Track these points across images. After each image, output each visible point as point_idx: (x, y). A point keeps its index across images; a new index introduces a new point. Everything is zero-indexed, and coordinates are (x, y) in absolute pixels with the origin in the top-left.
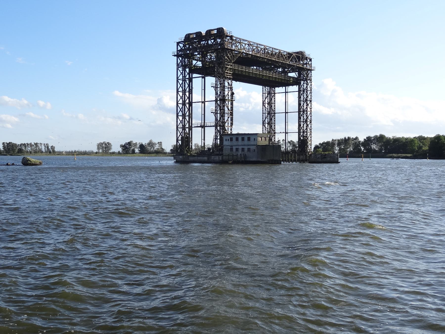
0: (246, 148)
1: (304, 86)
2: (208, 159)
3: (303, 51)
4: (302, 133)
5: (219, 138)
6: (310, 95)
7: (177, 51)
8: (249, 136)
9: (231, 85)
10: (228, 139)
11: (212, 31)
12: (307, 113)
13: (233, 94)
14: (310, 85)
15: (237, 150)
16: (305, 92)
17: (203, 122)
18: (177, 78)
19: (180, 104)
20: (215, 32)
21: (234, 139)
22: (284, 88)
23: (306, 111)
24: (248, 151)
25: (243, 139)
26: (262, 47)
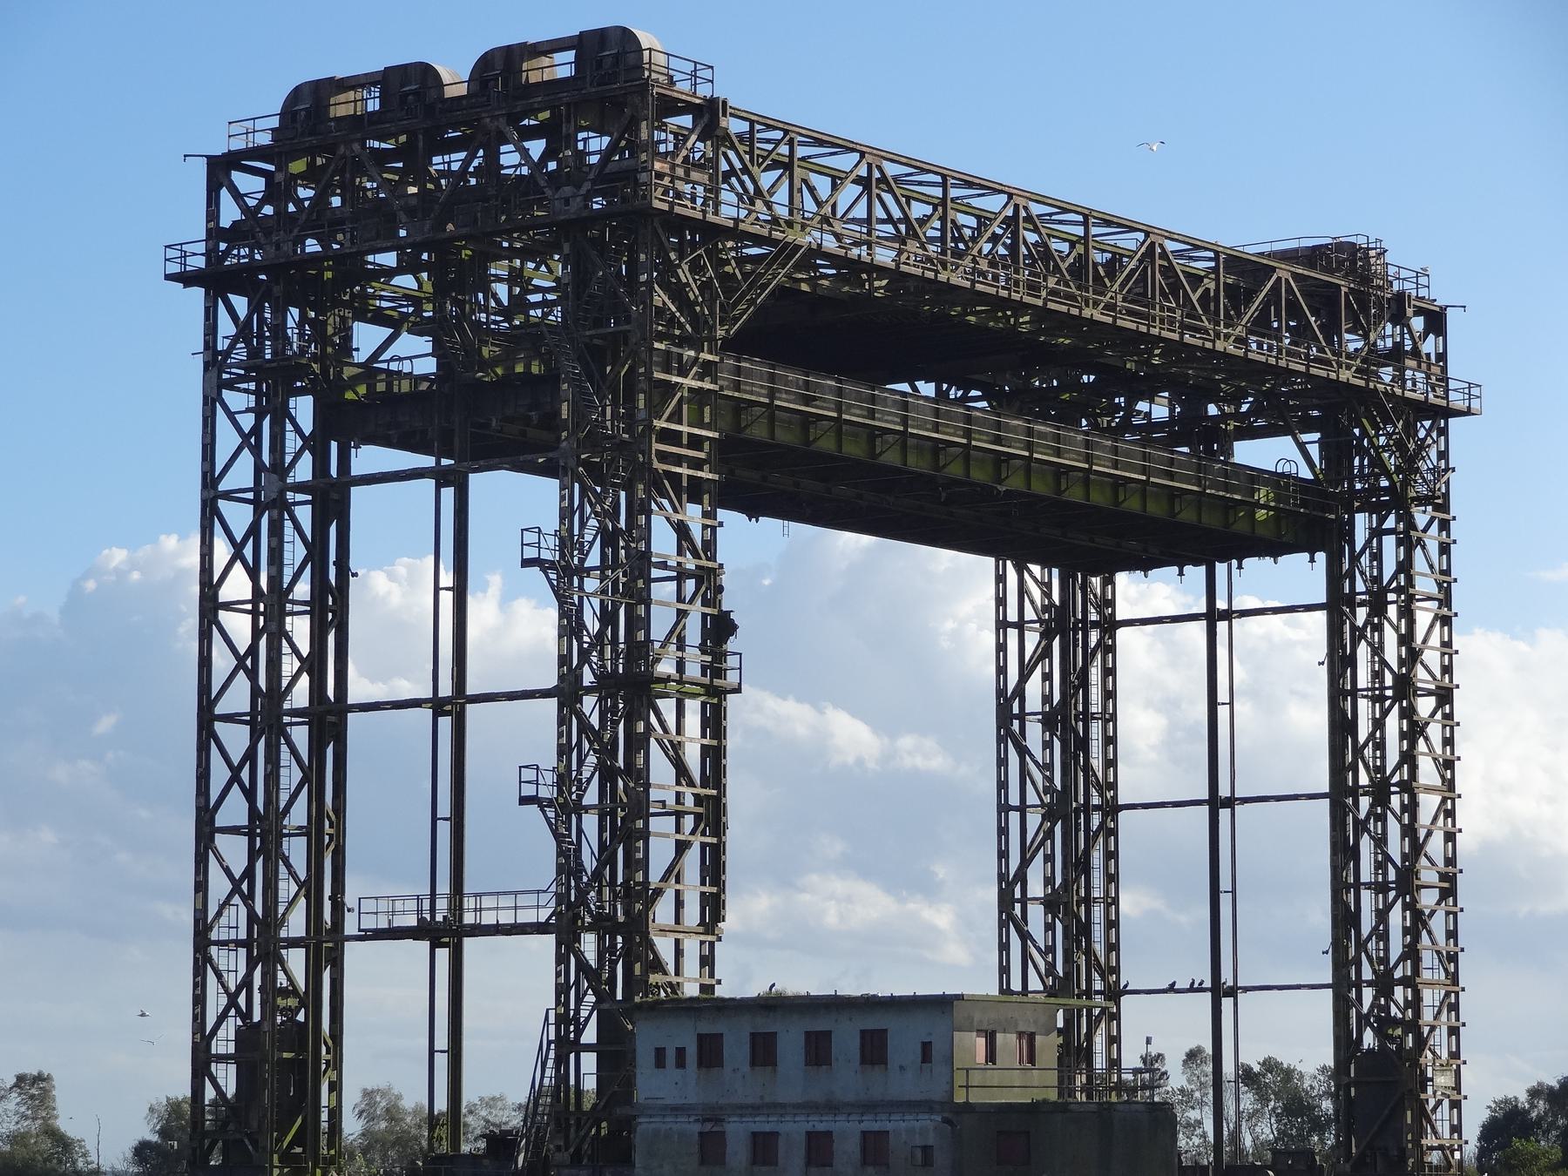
0: (848, 1131)
1: (1377, 557)
3: (1361, 241)
4: (1368, 994)
5: (590, 1035)
6: (1435, 640)
7: (214, 233)
8: (872, 1022)
9: (710, 546)
10: (681, 1052)
11: (535, 63)
12: (1411, 808)
13: (720, 628)
14: (1433, 547)
16: (1392, 611)
17: (444, 887)
18: (210, 480)
19: (229, 718)
20: (562, 66)
21: (736, 1050)
22: (1196, 574)
23: (1408, 787)
24: (865, 1162)
25: (818, 1050)
26: (994, 203)
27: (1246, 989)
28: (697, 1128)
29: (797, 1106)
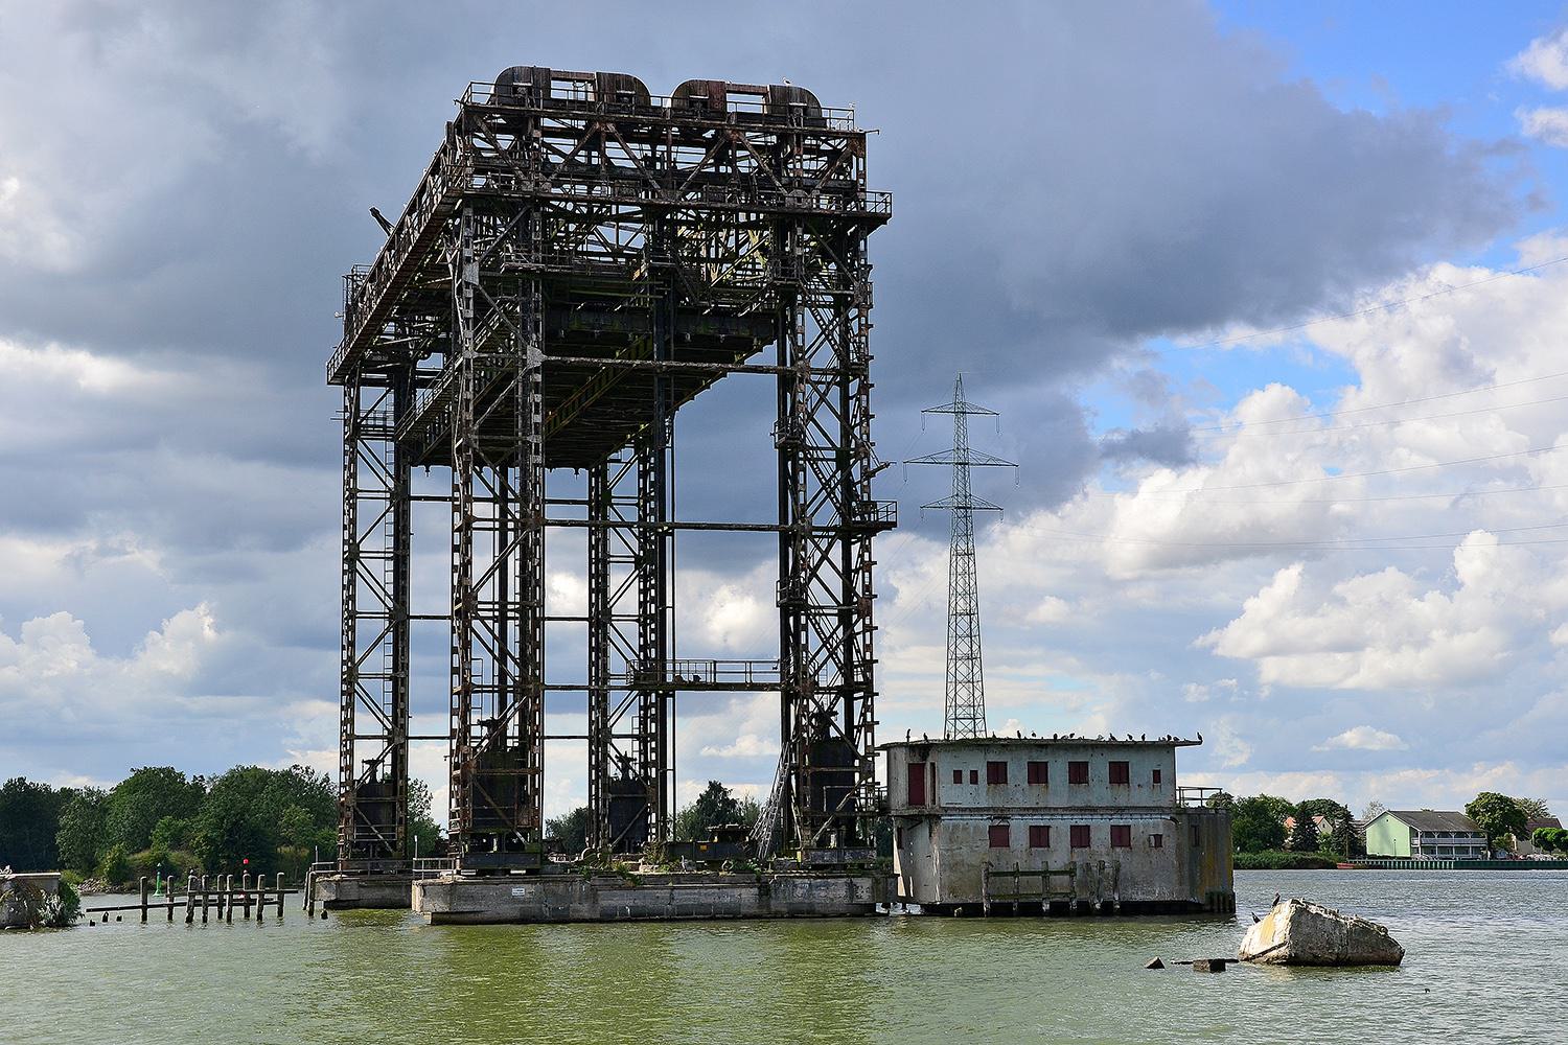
0: (1101, 828)
15: (1039, 837)
20: (755, 105)
21: (1017, 771)
27: (359, 737)
28: (989, 823)
29: (1064, 809)
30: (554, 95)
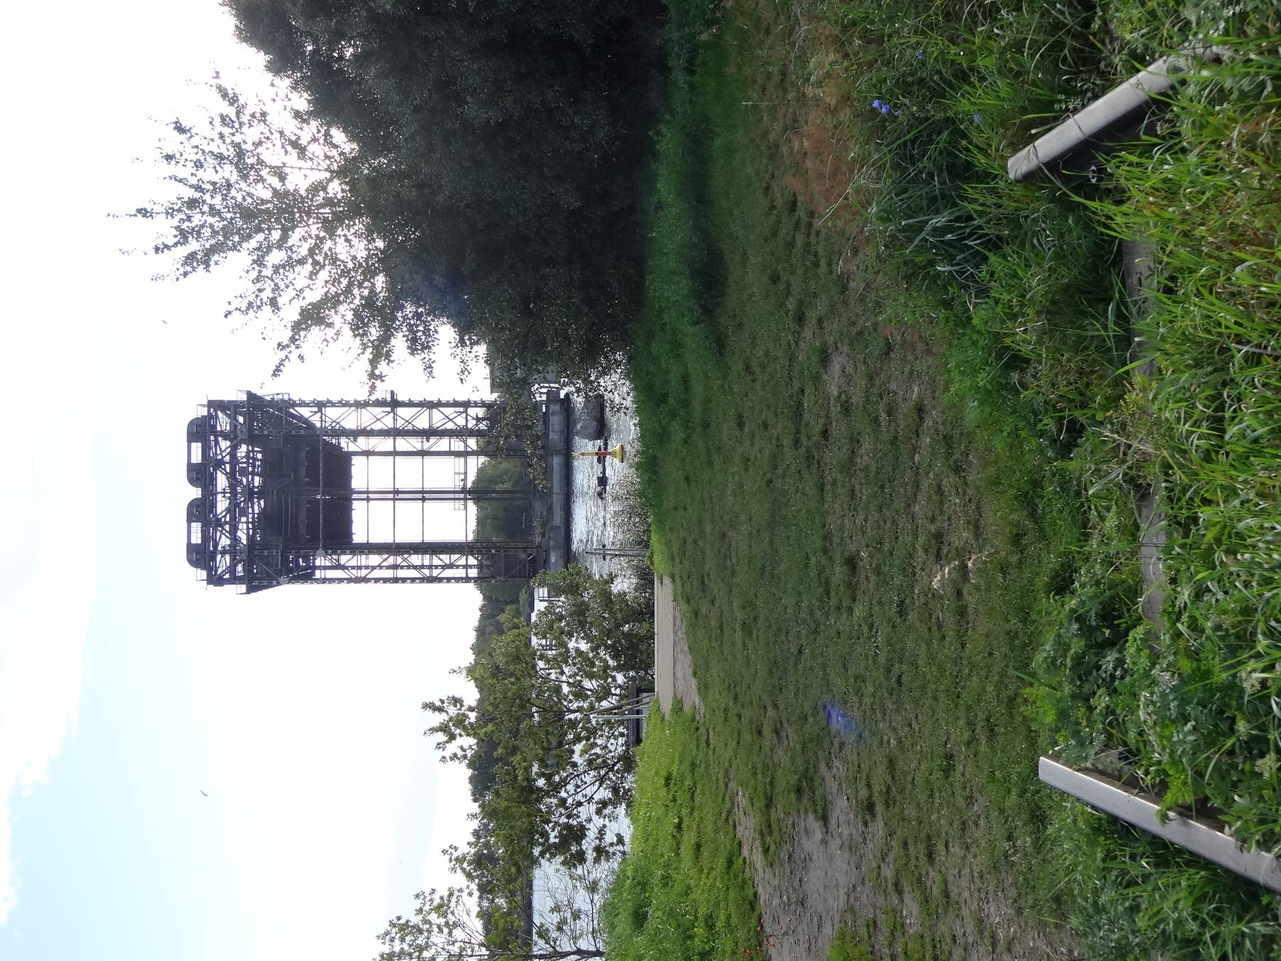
2: (558, 453)
20: (197, 448)
30: (199, 541)
